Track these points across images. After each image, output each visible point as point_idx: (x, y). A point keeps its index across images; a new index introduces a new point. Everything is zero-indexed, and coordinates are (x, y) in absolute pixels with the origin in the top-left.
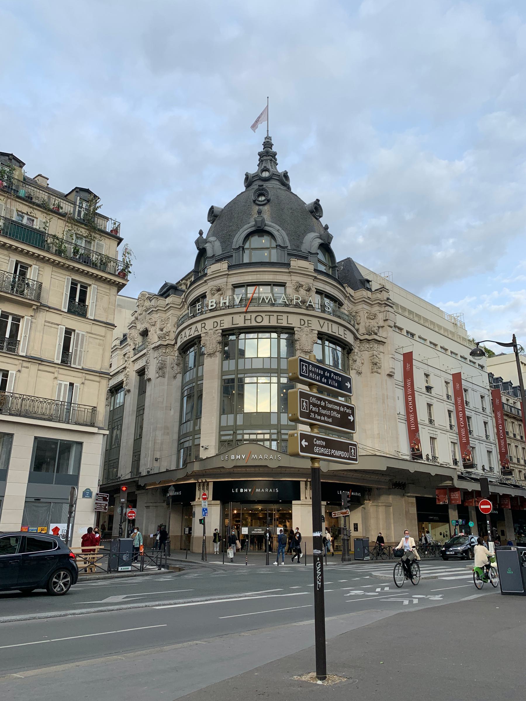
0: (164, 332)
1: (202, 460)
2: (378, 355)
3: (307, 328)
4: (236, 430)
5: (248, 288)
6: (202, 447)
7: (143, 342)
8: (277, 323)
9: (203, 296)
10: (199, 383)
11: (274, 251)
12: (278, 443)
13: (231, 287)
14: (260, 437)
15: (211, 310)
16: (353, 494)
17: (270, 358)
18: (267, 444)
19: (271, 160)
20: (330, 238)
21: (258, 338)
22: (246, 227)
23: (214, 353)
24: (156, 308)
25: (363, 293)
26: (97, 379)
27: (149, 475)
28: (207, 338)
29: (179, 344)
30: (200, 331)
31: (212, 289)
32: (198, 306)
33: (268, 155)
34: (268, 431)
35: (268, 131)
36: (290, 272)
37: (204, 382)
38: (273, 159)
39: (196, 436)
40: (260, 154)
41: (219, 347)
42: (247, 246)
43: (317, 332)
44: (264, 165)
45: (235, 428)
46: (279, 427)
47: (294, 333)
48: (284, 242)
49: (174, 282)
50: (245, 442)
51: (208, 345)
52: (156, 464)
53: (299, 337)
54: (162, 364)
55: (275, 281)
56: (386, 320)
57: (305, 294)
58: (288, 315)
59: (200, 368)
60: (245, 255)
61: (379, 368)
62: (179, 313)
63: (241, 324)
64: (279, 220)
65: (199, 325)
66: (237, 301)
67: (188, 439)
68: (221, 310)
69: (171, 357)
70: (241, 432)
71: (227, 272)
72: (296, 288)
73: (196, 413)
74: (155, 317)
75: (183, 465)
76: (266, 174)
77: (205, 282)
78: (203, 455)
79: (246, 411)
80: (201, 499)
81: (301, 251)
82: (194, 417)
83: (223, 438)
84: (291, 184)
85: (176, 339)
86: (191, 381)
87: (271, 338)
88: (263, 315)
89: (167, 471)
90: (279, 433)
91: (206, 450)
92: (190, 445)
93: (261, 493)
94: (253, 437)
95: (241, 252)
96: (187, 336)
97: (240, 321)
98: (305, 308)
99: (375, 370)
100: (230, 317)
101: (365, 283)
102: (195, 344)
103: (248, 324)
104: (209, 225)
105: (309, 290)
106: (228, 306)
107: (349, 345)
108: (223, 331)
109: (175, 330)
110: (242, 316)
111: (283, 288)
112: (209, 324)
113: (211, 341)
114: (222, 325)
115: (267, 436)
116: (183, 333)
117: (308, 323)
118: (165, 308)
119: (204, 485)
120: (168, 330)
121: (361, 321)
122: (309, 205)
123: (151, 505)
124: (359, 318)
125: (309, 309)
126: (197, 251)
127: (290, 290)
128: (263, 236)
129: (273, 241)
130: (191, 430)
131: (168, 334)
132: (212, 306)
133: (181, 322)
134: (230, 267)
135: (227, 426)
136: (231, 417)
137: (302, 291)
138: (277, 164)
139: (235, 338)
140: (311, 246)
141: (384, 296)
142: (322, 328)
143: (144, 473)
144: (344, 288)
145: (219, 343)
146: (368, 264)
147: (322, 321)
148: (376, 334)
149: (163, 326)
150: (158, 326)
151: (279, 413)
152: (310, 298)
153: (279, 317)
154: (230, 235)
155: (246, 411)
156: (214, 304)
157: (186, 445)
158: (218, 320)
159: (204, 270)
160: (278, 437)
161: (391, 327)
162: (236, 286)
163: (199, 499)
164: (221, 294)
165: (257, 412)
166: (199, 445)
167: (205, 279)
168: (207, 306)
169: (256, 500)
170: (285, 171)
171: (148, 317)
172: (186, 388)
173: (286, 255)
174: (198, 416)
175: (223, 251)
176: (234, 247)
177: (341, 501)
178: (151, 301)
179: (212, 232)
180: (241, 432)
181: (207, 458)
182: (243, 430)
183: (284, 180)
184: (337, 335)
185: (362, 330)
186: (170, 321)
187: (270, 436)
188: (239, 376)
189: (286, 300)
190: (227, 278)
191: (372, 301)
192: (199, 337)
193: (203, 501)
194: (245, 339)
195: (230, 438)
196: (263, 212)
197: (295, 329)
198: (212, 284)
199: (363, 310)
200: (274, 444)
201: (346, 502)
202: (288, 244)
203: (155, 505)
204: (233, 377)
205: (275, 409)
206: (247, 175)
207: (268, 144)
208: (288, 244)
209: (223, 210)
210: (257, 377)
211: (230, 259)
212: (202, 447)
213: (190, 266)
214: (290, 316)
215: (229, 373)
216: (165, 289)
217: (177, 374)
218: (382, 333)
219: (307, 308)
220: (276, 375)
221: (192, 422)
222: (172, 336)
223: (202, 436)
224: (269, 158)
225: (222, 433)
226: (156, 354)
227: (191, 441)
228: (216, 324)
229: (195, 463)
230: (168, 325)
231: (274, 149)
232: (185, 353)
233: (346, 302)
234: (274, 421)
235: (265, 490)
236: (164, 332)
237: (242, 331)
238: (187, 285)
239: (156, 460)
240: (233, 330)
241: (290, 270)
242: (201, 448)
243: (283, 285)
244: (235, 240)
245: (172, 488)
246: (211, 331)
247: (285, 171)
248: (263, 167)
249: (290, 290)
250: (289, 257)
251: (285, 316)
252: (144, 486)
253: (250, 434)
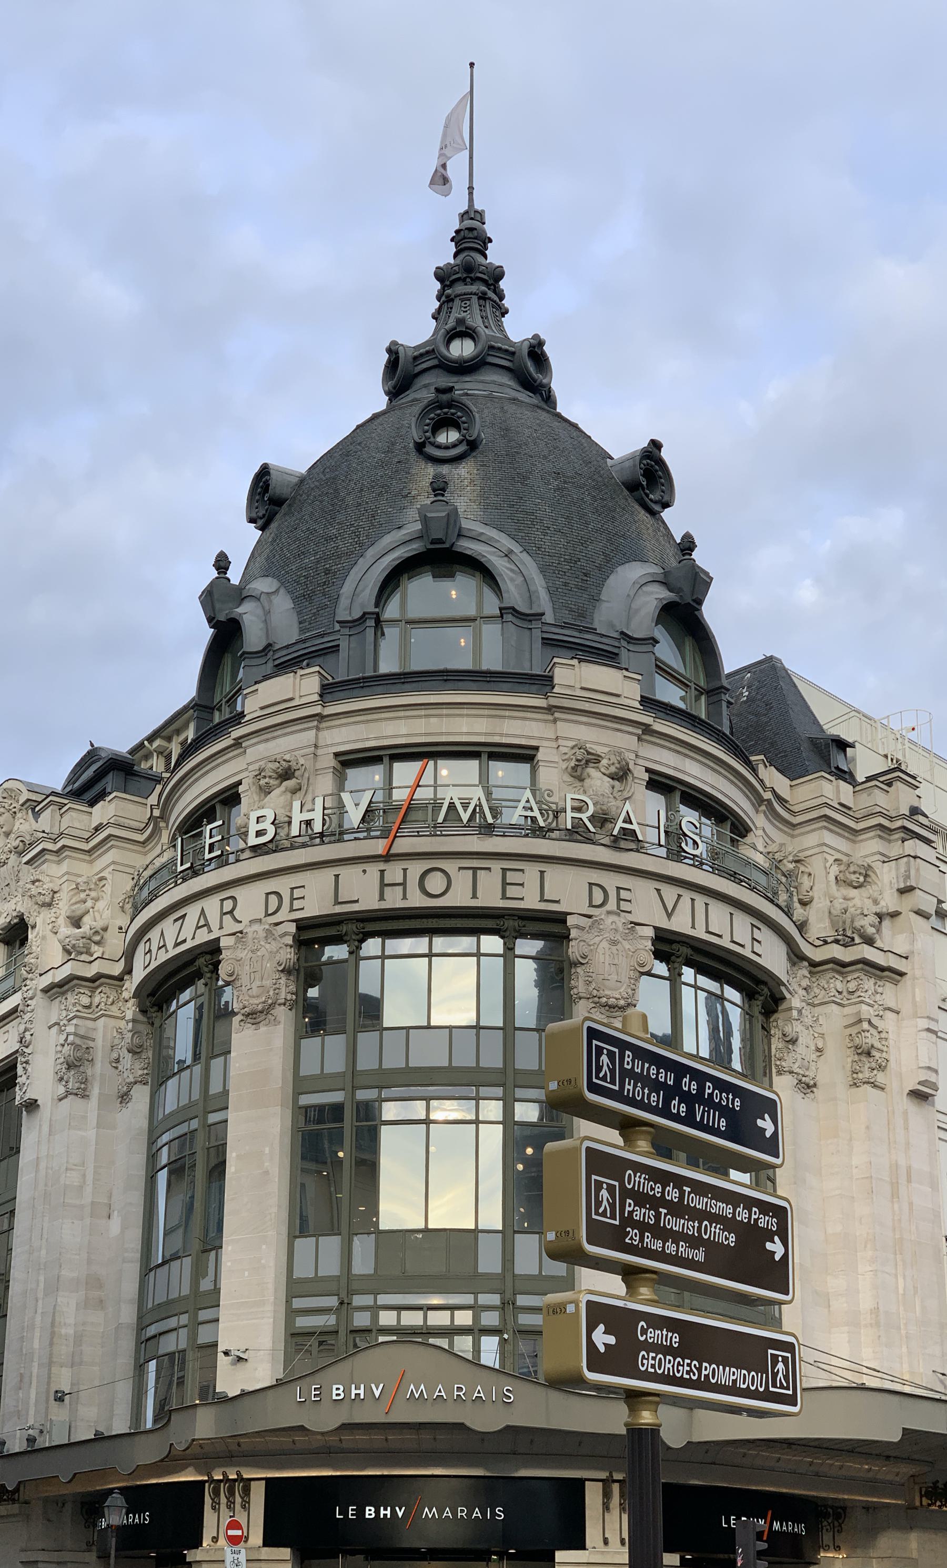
0: (85, 929)
1: (225, 1400)
2: (875, 1021)
3: (613, 918)
4: (351, 1293)
5: (396, 765)
6: (226, 1353)
7: (8, 965)
8: (504, 897)
9: (230, 797)
10: (213, 1118)
11: (492, 632)
12: (503, 1342)
13: (332, 762)
14: (439, 1319)
15: (258, 850)
16: (776, 1526)
17: (478, 1027)
18: (464, 1344)
19: (483, 297)
20: (699, 582)
21: (430, 955)
22: (387, 540)
23: (267, 1010)
24: (55, 841)
25: (822, 789)
27: (33, 1450)
28: (242, 954)
29: (139, 974)
30: (214, 925)
31: (261, 770)
32: (210, 832)
33: (470, 277)
34: (468, 1299)
35: (471, 189)
36: (550, 709)
37: (232, 1116)
38: (491, 294)
39: (203, 1315)
40: (442, 275)
41: (286, 988)
42: (392, 610)
43: (650, 932)
44: (456, 314)
45: (346, 1287)
46: (508, 1284)
47: (566, 937)
48: (531, 596)
49: (122, 745)
50: (381, 1339)
51: (244, 980)
52: (59, 1414)
53: (585, 950)
54: (77, 1047)
55: (497, 739)
56: (905, 891)
57: (608, 791)
58: (543, 867)
59: (217, 1063)
60: (383, 644)
61: (881, 1068)
62: (138, 860)
63: (369, 902)
64: (512, 514)
65: (212, 905)
66: (354, 816)
67: (172, 1322)
68: (292, 847)
69: (112, 1022)
70: (367, 1300)
71: (318, 709)
72: (574, 768)
73: (201, 1232)
74: (53, 873)
75: (155, 1421)
76: (462, 349)
77: (237, 743)
78: (229, 1382)
79: (382, 1227)
80: (222, 1542)
81: (593, 631)
82: (196, 1246)
83: (303, 1322)
84: (558, 384)
85: (129, 955)
86: (183, 1114)
87: (478, 955)
88: (450, 866)
89: (100, 1438)
90: (507, 1306)
91: (239, 1365)
92: (182, 1345)
93: (441, 1521)
94: (412, 1319)
95: (370, 633)
96: (170, 945)
97: (363, 891)
98: (606, 841)
99: (866, 1074)
100: (328, 875)
101: (830, 753)
102: (198, 975)
103: (394, 900)
104: (253, 534)
105: (621, 775)
106: (322, 835)
107: (771, 983)
108: (303, 925)
109: (124, 921)
110: (373, 870)
111: (526, 767)
112: (250, 901)
113: (257, 965)
114: (297, 904)
115: (464, 1318)
116: (154, 934)
117: (619, 899)
118: (87, 840)
119: (231, 1492)
120: (99, 925)
121: (815, 893)
122: (623, 461)
123: (40, 1556)
124: (806, 882)
125: (623, 844)
126: (207, 633)
127: (552, 774)
128: (452, 575)
129: (488, 593)
130: (186, 1291)
131: (99, 936)
132: (259, 834)
133: (145, 893)
134: (328, 691)
135: (317, 1279)
136: (331, 1245)
137: (598, 781)
138: (505, 312)
139: (345, 955)
140: (630, 613)
141: (900, 799)
142: (669, 915)
143: (16, 1445)
144: (754, 770)
145: (287, 971)
146: (838, 685)
147: (670, 893)
148: (870, 941)
149: (81, 908)
150: (64, 907)
151: (508, 1233)
152: (628, 807)
153: (510, 878)
154: (327, 572)
155: (382, 1227)
156: (267, 825)
157: (169, 1344)
158: (282, 884)
159: (232, 701)
160: (503, 1319)
161: (926, 916)
162: (350, 760)
163: (215, 1539)
164: (295, 791)
165: (426, 1230)
166: (215, 1345)
167: (237, 733)
168: (244, 835)
169: (423, 1545)
170: (536, 336)
171: (28, 874)
172: (165, 1138)
173: (538, 644)
174: (211, 1242)
175: (302, 631)
176: (343, 615)
177: (734, 1552)
178: (37, 815)
179: (264, 561)
180: (367, 1300)
181: (244, 1394)
182: (376, 1294)
183: (529, 368)
184: (725, 943)
185: (819, 927)
186: (108, 889)
187: (476, 1318)
188: (362, 1095)
189: (536, 813)
190: (318, 728)
191: (857, 820)
192: (212, 950)
193: (228, 1550)
194: (383, 957)
195: (330, 1320)
196: (451, 487)
197: (571, 921)
198: (259, 753)
199: (822, 853)
200: (490, 1344)
201: (752, 1554)
202: (544, 603)
203: (55, 1556)
204: (336, 1097)
205: (493, 1218)
206: (393, 352)
207: (471, 237)
208: (544, 603)
209: (302, 480)
210: (428, 1099)
211: (330, 658)
212: (226, 1353)
213: (184, 686)
214: (554, 874)
215: (321, 1082)
216: (90, 773)
217: (131, 1085)
218: (893, 939)
219: (615, 844)
220: (499, 1091)
221: (187, 1261)
222: (116, 944)
223: (224, 1313)
224: (473, 288)
225: (298, 1303)
226: (56, 1011)
227: (183, 1333)
228: (273, 900)
229: (200, 1412)
230: (100, 905)
231: (494, 256)
232: (160, 1009)
233: (758, 821)
234: (489, 1260)
235: (454, 1513)
236: (85, 929)
237: (371, 927)
238: (168, 757)
239: (60, 1397)
240: (339, 923)
241: (553, 701)
242: (220, 1356)
243: (524, 755)
244: (347, 589)
245: (117, 1499)
246: (256, 927)
247: (536, 336)
248: (451, 323)
249: (552, 774)
250: (550, 651)
251: (532, 871)
252: (17, 1490)
253: (399, 1308)
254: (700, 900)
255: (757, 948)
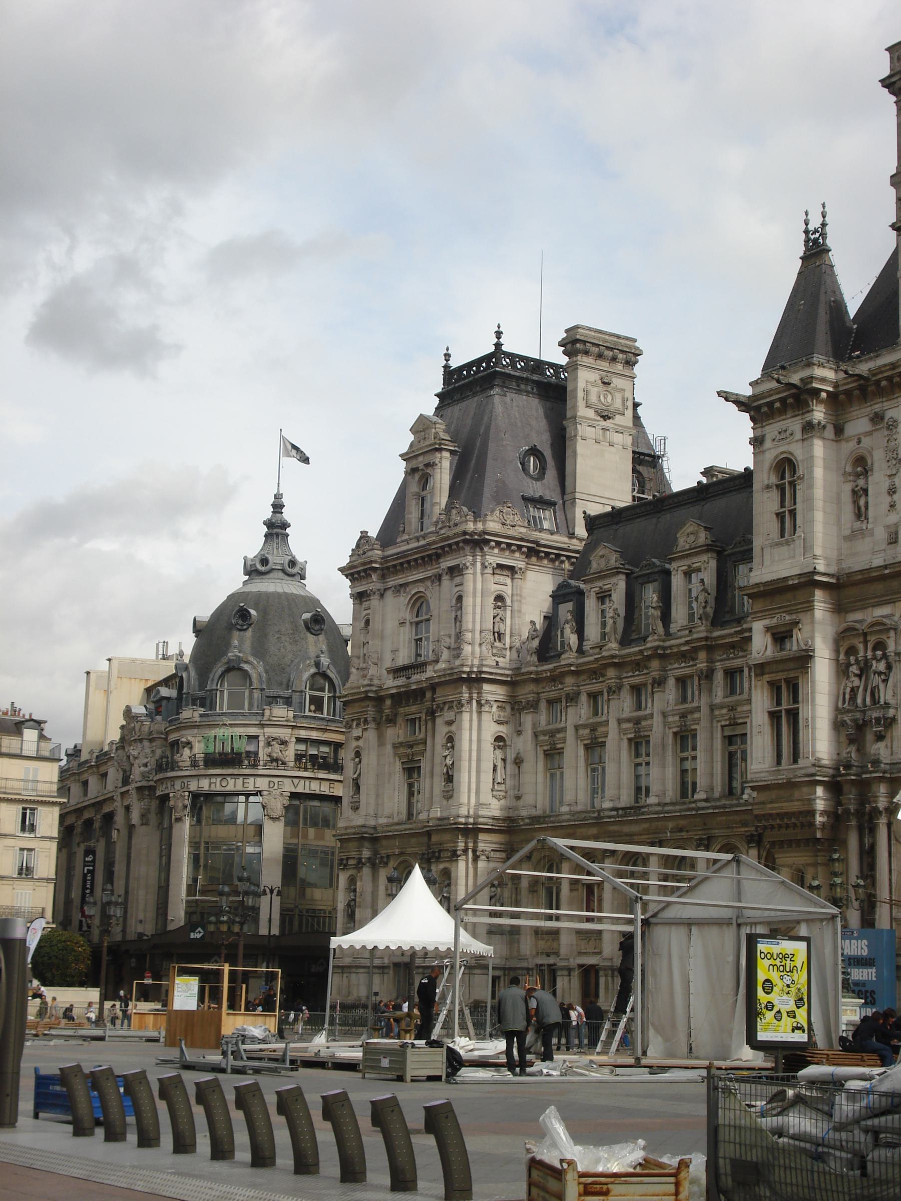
26: (45, 884)
63: (206, 788)
88: (229, 779)
147: (296, 781)
158: (185, 780)
184: (318, 792)
214: (259, 780)
251: (252, 780)
254: (307, 782)
255: (332, 790)
